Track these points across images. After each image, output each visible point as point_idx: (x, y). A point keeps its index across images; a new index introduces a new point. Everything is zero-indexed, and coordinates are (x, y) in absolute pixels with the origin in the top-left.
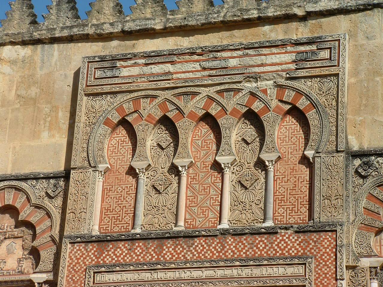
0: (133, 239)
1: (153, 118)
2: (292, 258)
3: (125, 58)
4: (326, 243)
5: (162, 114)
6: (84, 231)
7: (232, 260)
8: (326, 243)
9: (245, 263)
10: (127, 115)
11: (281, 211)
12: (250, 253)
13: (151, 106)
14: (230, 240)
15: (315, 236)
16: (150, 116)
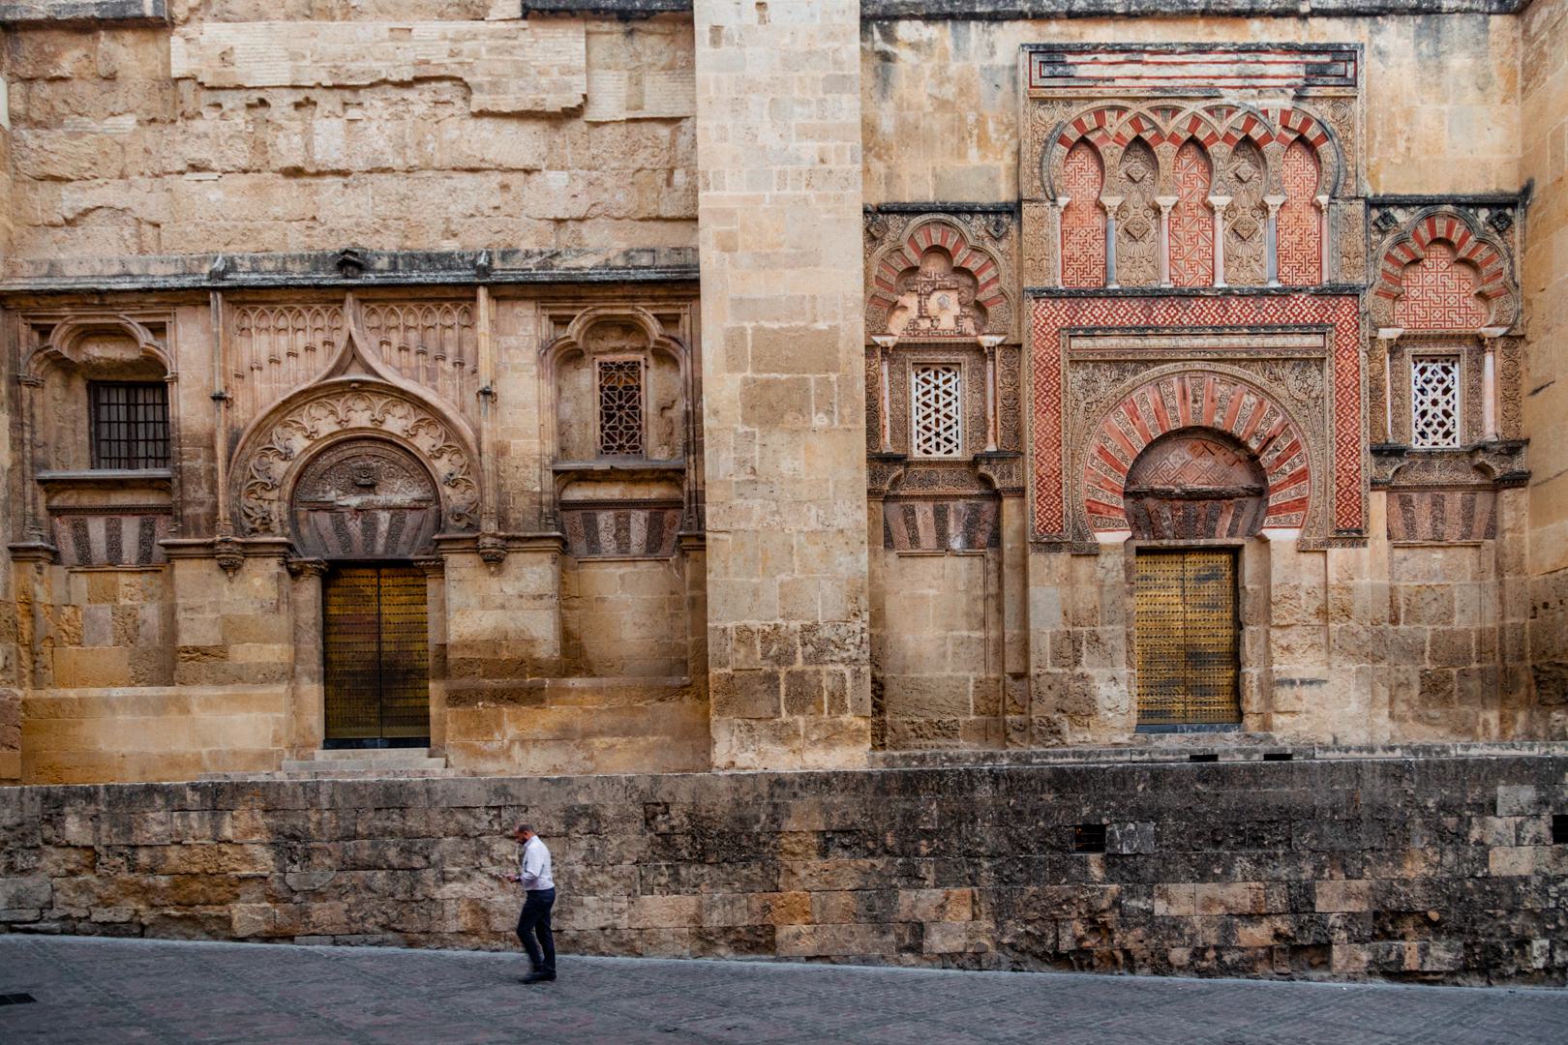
0: (1113, 296)
1: (1124, 139)
2: (1309, 326)
3: (1081, 50)
4: (1346, 309)
5: (1134, 134)
6: (1048, 284)
7: (1239, 328)
8: (1346, 309)
9: (1254, 330)
10: (1089, 132)
11: (1286, 269)
12: (1259, 319)
13: (1121, 121)
14: (1234, 302)
15: (1334, 302)
16: (1118, 135)
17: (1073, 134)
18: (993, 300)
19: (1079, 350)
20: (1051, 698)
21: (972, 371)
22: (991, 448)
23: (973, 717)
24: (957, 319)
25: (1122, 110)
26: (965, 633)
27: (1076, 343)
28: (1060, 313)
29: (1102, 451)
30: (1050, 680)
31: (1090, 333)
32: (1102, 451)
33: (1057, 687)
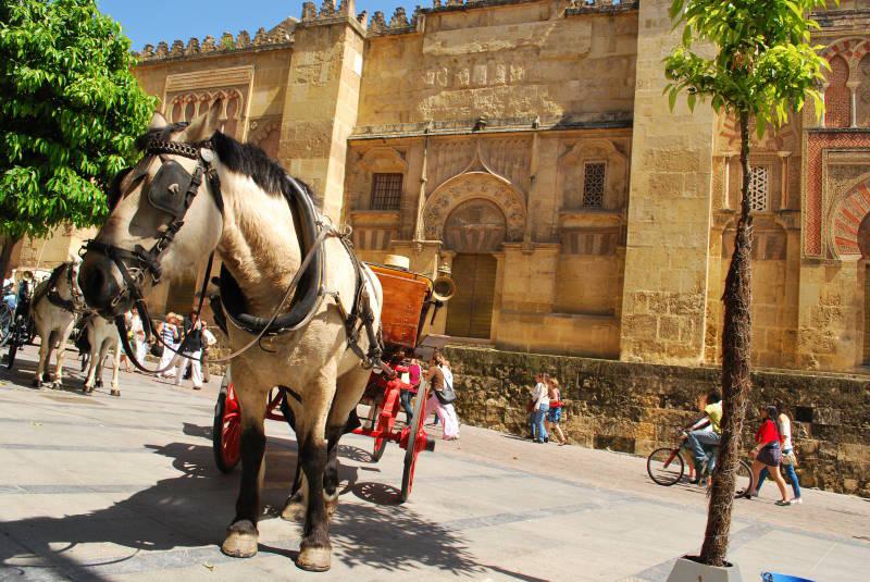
17: (833, 54)
18: (784, 135)
19: (833, 160)
20: (810, 343)
21: (774, 169)
22: (783, 207)
23: (766, 351)
24: (767, 143)
25: (858, 41)
26: (765, 305)
27: (831, 156)
28: (824, 143)
29: (845, 211)
30: (809, 333)
31: (840, 150)
32: (845, 211)
33: (813, 337)
